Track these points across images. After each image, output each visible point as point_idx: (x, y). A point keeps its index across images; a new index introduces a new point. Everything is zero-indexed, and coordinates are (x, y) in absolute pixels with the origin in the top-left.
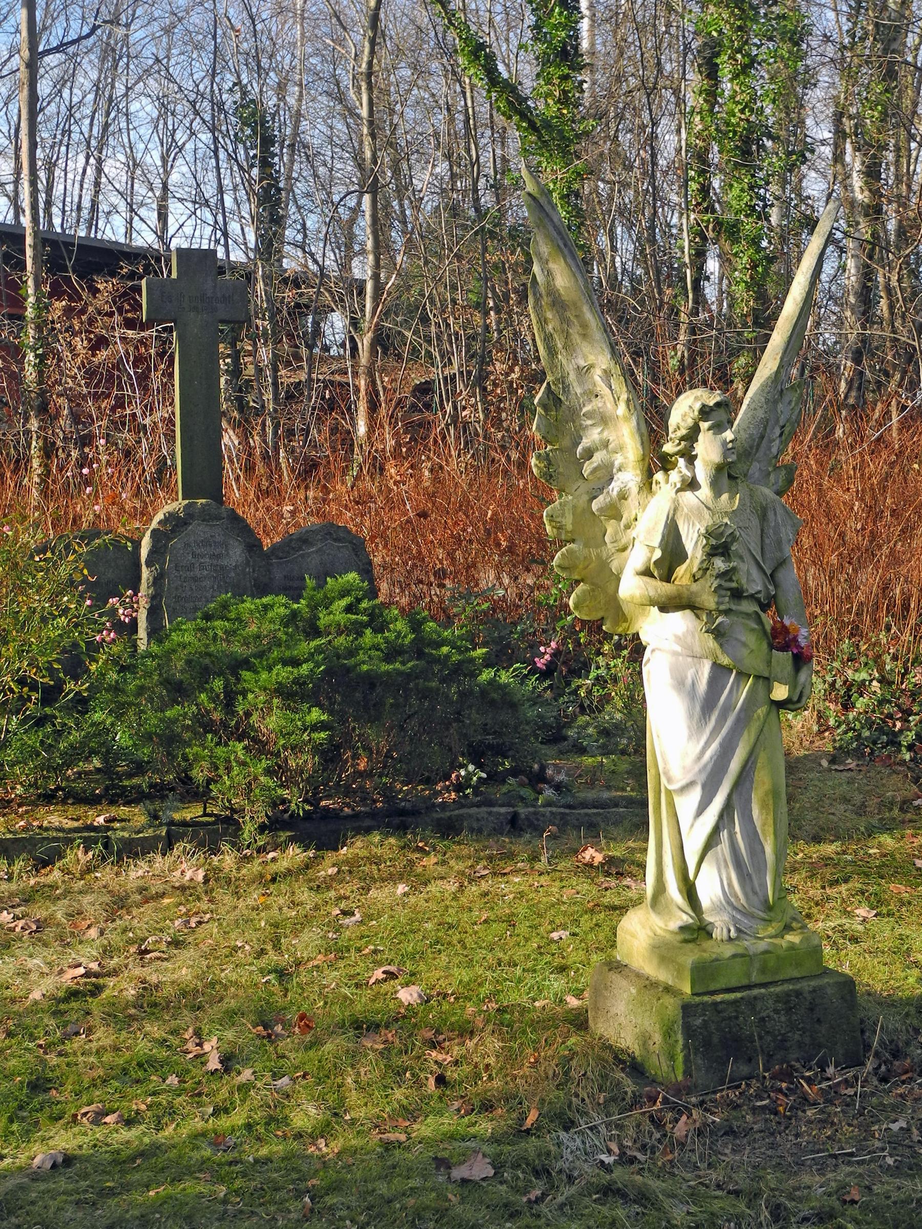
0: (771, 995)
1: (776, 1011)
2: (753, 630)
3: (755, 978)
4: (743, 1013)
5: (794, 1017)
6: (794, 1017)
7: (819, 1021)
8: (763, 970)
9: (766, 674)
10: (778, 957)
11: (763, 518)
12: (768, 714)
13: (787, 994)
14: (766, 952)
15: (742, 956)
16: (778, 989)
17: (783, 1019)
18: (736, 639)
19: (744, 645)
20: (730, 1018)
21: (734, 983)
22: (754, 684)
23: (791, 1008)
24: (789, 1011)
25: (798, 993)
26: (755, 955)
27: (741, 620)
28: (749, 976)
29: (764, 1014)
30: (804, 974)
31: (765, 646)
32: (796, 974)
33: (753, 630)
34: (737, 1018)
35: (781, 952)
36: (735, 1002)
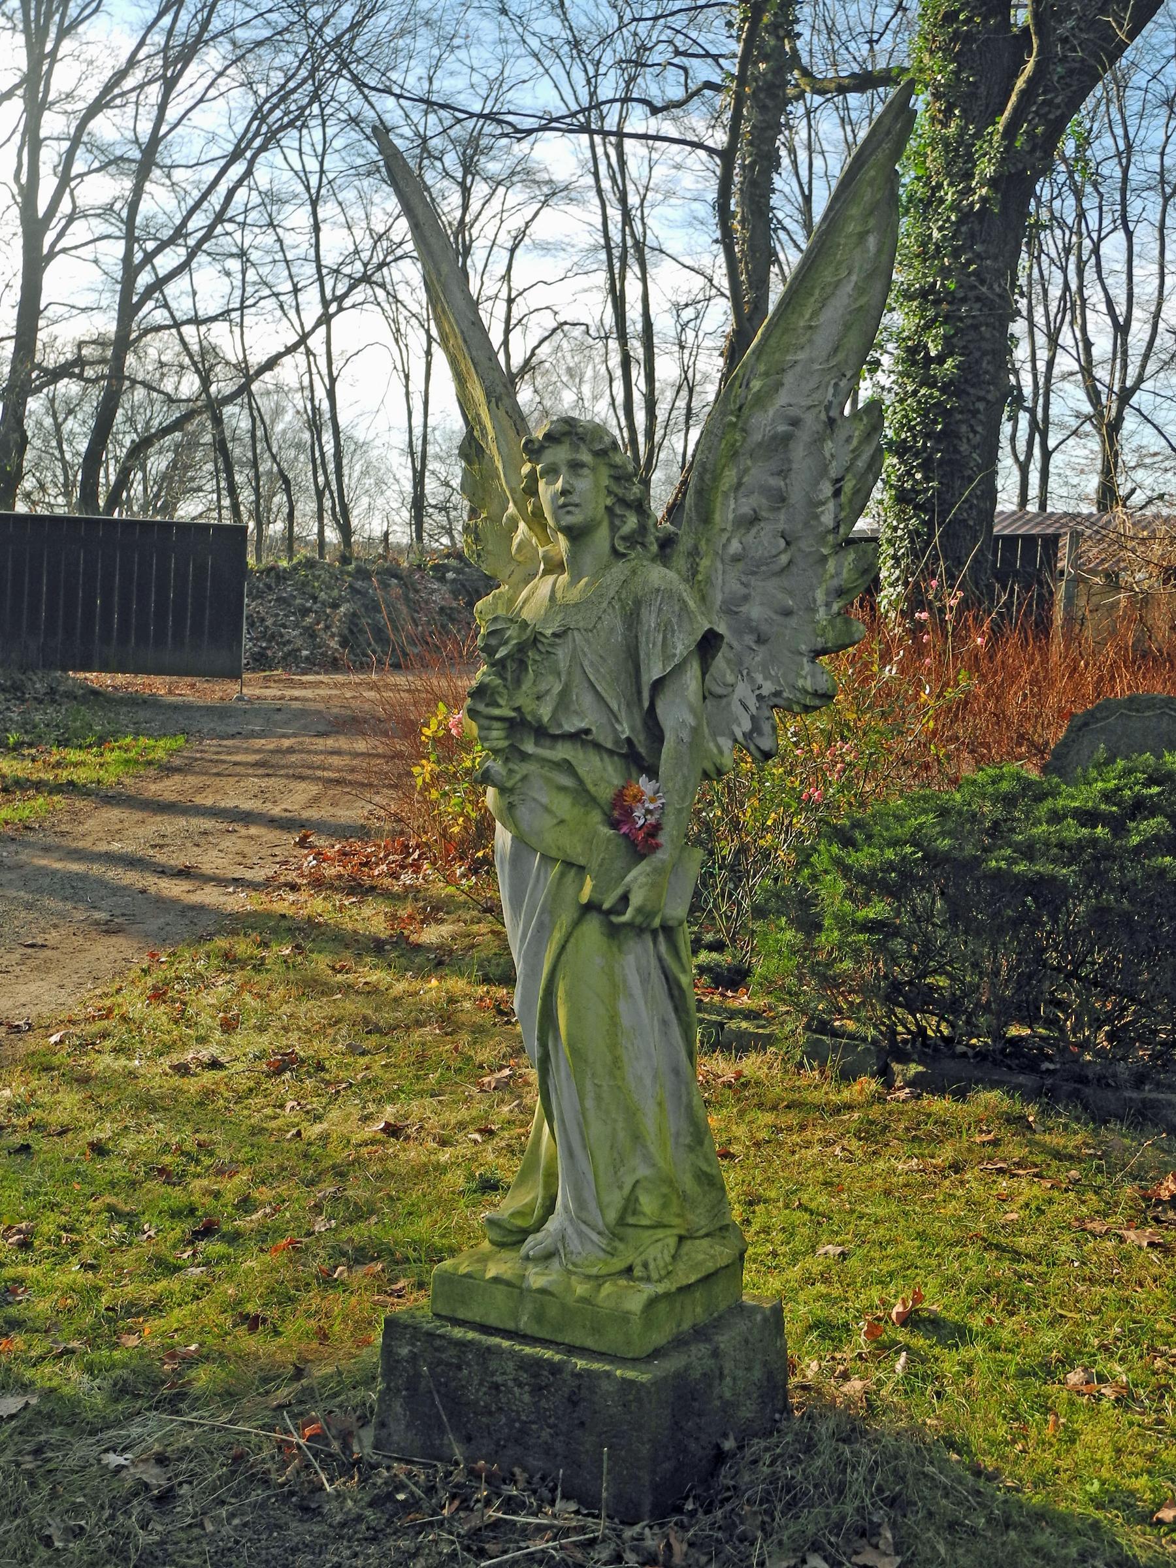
0: (512, 1353)
1: (520, 1385)
2: (562, 789)
3: (525, 1323)
4: (468, 1365)
5: (543, 1403)
6: (543, 1403)
7: (582, 1424)
8: (539, 1317)
9: (582, 861)
10: (563, 1306)
11: (632, 619)
12: (577, 923)
13: (539, 1362)
14: (543, 1291)
15: (508, 1284)
16: (528, 1350)
17: (527, 1398)
18: (534, 800)
19: (547, 809)
20: (448, 1364)
21: (493, 1320)
22: (562, 875)
23: (541, 1389)
24: (537, 1390)
25: (555, 1369)
26: (529, 1290)
27: (545, 771)
28: (516, 1319)
29: (498, 1379)
30: (604, 1350)
31: (596, 817)
32: (589, 1343)
33: (562, 789)
34: (459, 1368)
35: (570, 1301)
36: (462, 1344)
